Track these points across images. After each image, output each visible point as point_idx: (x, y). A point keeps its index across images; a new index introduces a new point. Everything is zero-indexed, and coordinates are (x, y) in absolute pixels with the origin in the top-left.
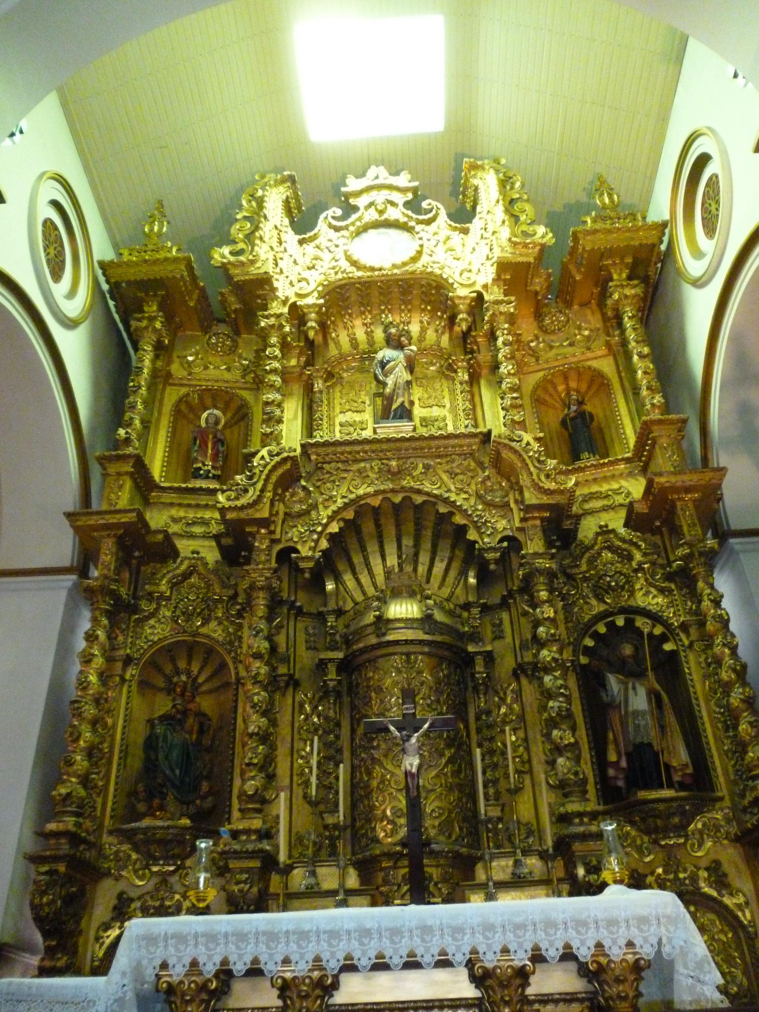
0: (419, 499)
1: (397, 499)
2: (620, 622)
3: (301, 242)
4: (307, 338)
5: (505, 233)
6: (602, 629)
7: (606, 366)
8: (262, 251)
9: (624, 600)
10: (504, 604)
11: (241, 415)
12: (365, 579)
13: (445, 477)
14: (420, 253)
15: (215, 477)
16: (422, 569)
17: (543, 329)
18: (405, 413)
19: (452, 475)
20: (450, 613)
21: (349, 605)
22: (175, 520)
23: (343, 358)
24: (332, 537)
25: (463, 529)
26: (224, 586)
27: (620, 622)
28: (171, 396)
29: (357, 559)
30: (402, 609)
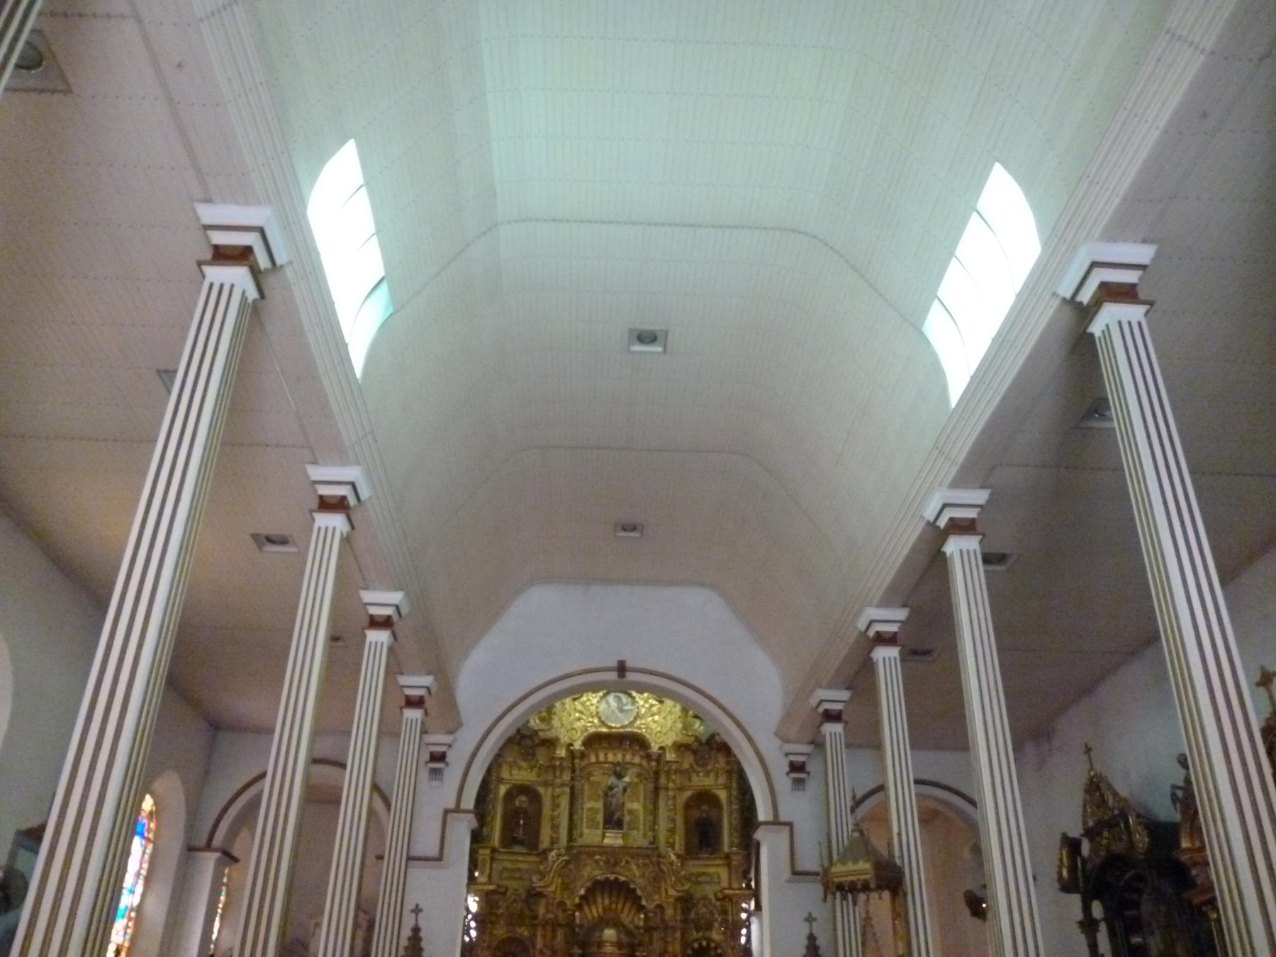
0: (622, 879)
1: (612, 877)
2: (704, 943)
3: (575, 699)
4: (573, 764)
5: (680, 726)
6: (696, 945)
7: (722, 795)
8: (556, 722)
9: (708, 934)
10: (655, 929)
11: (535, 798)
12: (594, 910)
13: (634, 867)
14: (635, 719)
15: (521, 843)
16: (620, 906)
17: (696, 760)
18: (619, 824)
19: (638, 867)
20: (629, 933)
21: (585, 922)
22: (505, 869)
23: (591, 764)
24: (582, 898)
25: (640, 898)
26: (530, 910)
27: (704, 943)
28: (503, 790)
29: (591, 899)
30: (610, 933)
